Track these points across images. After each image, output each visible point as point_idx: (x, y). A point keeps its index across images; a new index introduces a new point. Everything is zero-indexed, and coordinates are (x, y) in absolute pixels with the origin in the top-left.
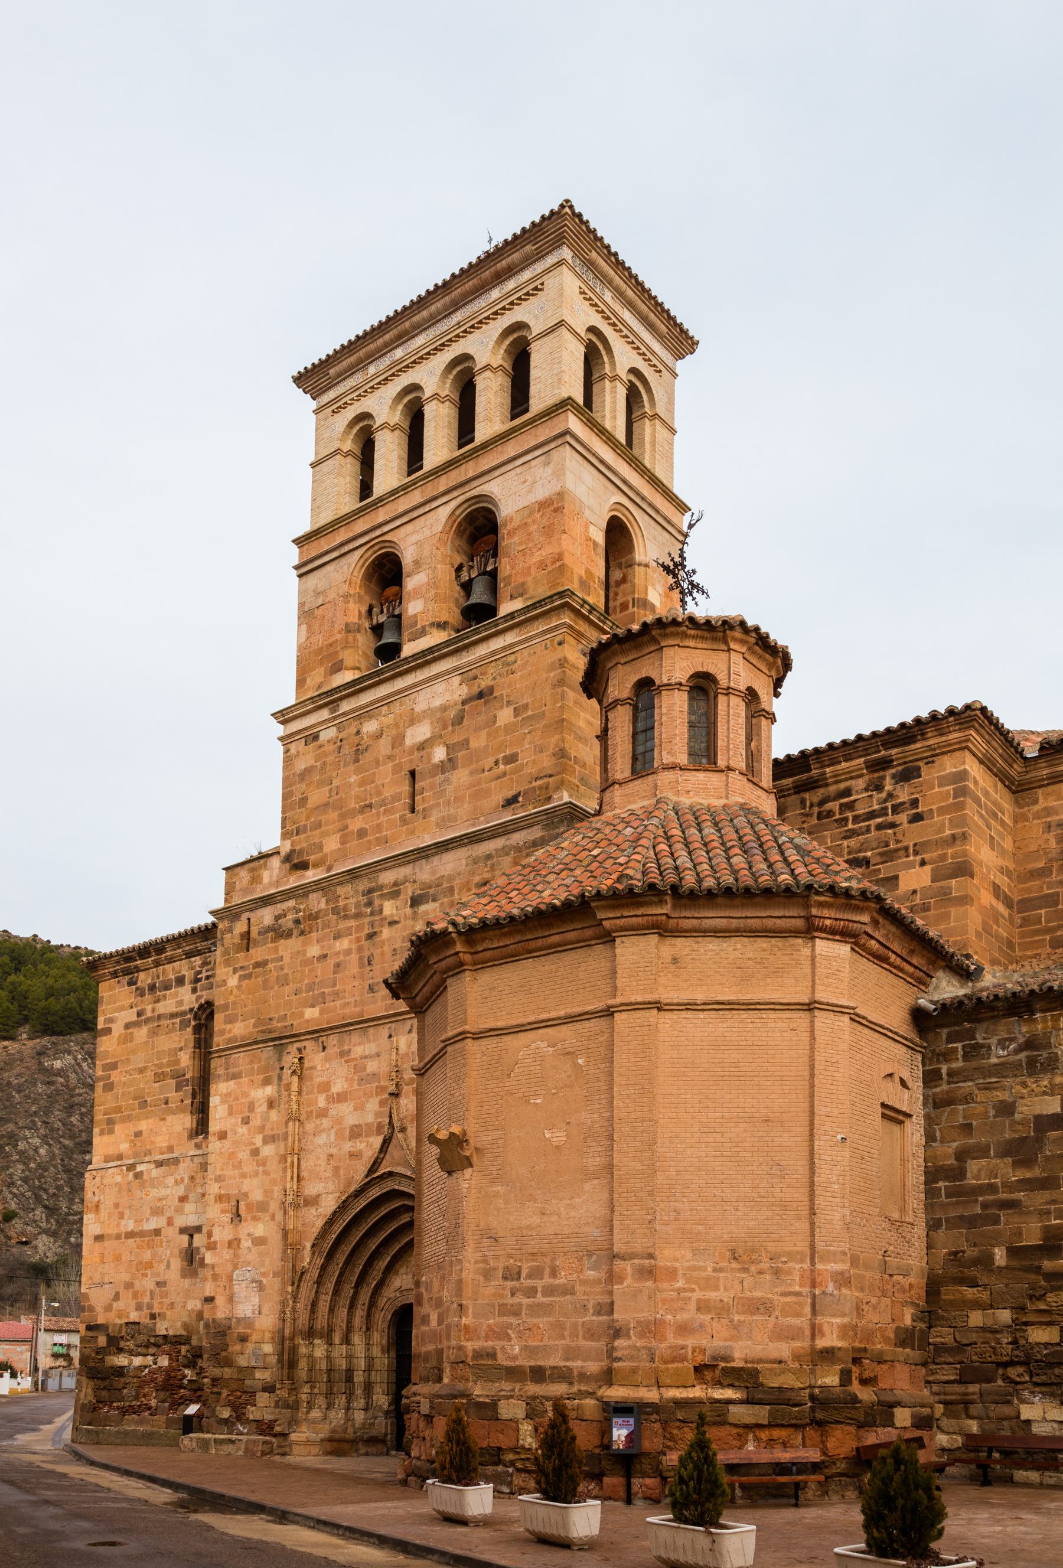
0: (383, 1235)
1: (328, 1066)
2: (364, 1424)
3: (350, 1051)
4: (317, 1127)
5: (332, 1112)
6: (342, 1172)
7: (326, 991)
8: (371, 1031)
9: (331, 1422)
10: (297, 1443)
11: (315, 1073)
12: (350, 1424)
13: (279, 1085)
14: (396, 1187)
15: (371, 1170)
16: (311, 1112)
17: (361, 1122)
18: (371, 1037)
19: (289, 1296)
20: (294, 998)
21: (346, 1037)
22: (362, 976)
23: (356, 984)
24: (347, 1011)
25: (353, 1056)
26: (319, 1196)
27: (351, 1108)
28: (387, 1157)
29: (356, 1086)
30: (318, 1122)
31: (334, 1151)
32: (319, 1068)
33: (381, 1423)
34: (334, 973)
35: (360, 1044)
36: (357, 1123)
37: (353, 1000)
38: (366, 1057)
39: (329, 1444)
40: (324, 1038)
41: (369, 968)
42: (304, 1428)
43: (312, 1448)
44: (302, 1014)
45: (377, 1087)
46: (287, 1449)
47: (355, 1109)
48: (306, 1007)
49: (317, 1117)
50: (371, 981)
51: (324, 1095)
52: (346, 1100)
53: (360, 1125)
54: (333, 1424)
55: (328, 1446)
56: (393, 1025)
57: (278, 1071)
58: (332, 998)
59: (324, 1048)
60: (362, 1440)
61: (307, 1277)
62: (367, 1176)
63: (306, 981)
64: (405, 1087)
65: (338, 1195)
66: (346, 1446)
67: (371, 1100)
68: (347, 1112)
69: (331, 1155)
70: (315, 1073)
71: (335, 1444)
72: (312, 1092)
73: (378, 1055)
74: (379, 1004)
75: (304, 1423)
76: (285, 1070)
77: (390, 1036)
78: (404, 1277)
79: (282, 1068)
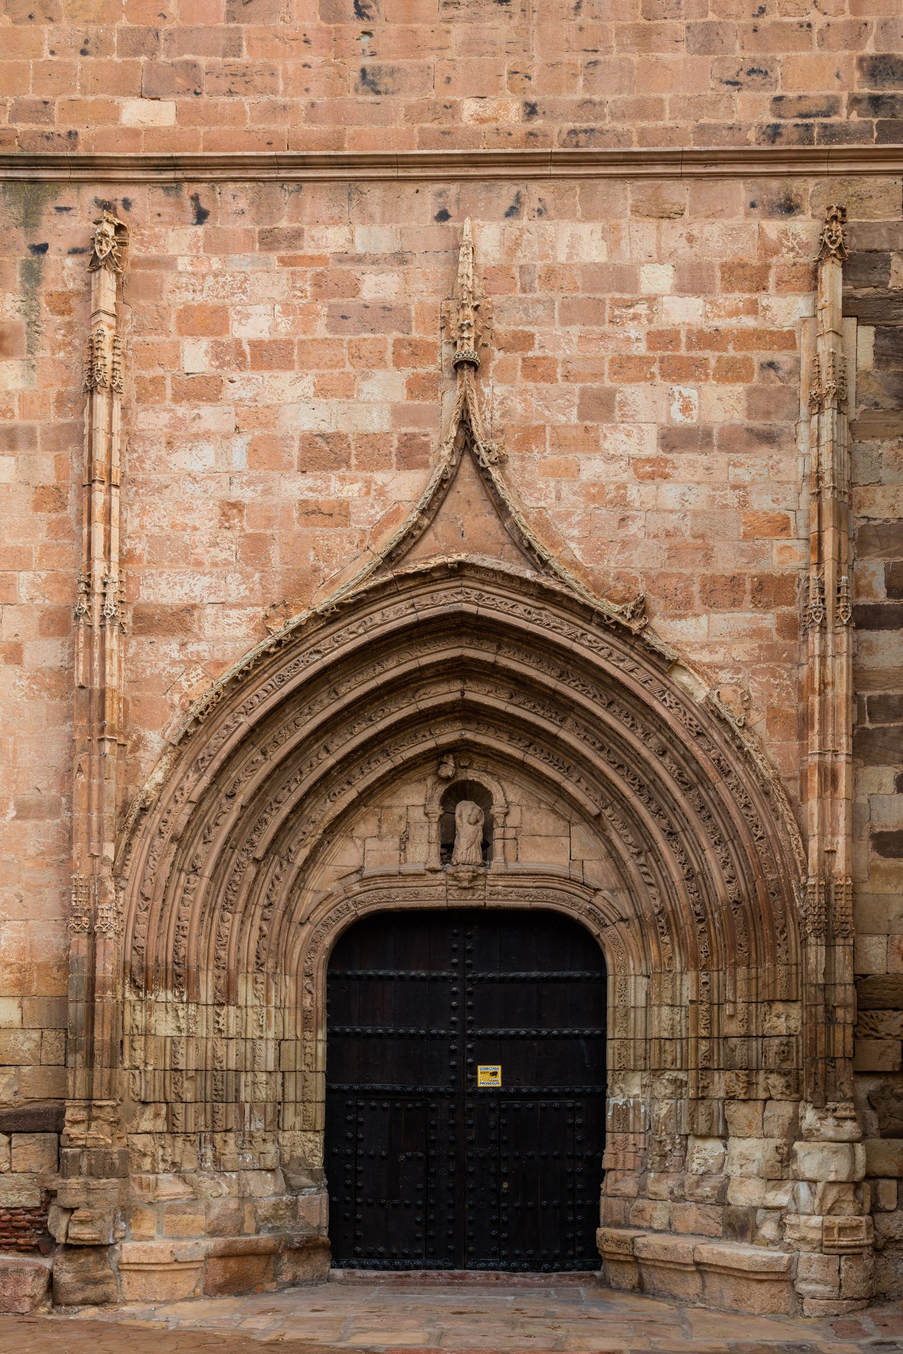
0: (363, 733)
1: (216, 263)
2: (276, 1207)
3: (298, 235)
4: (178, 423)
5: (231, 392)
6: (275, 553)
7: (203, 61)
8: (375, 193)
9: (209, 1207)
10: (140, 1269)
11: (169, 279)
12: (247, 1207)
13: (30, 294)
14: (471, 608)
15: (392, 558)
16: (157, 382)
17: (344, 428)
18: (376, 210)
19: (106, 871)
20: (78, 61)
21: (284, 197)
22: (336, 42)
23: (314, 59)
24: (282, 127)
25: (308, 249)
26: (190, 609)
27: (307, 385)
28: (440, 527)
29: (320, 330)
30: (183, 410)
31: (247, 495)
32: (183, 264)
33: (310, 1203)
34: (231, 16)
35: (335, 221)
36: (330, 430)
37: (302, 101)
38: (359, 259)
39: (220, 1264)
40: (201, 189)
41: (362, 25)
42: (147, 1226)
43: (180, 1277)
44: (114, 113)
45: (398, 343)
46: (110, 1288)
47: (322, 391)
48: (127, 92)
49: (177, 398)
50: (367, 62)
51: (205, 343)
52: (287, 364)
53: (340, 437)
54: (215, 1211)
55: (218, 1272)
56: (454, 189)
57: (25, 254)
58: (224, 84)
59: (201, 216)
60: (290, 1249)
61: (152, 822)
62: (378, 570)
63: (124, 22)
64: (499, 355)
65: (261, 612)
66: (254, 1266)
67: (379, 374)
68: (291, 394)
69: (237, 506)
70: (169, 279)
71: (232, 1263)
72: (159, 328)
73: (401, 258)
74: (400, 125)
75: (149, 1213)
76: (51, 255)
77: (443, 216)
78: (372, 844)
79: (42, 249)
